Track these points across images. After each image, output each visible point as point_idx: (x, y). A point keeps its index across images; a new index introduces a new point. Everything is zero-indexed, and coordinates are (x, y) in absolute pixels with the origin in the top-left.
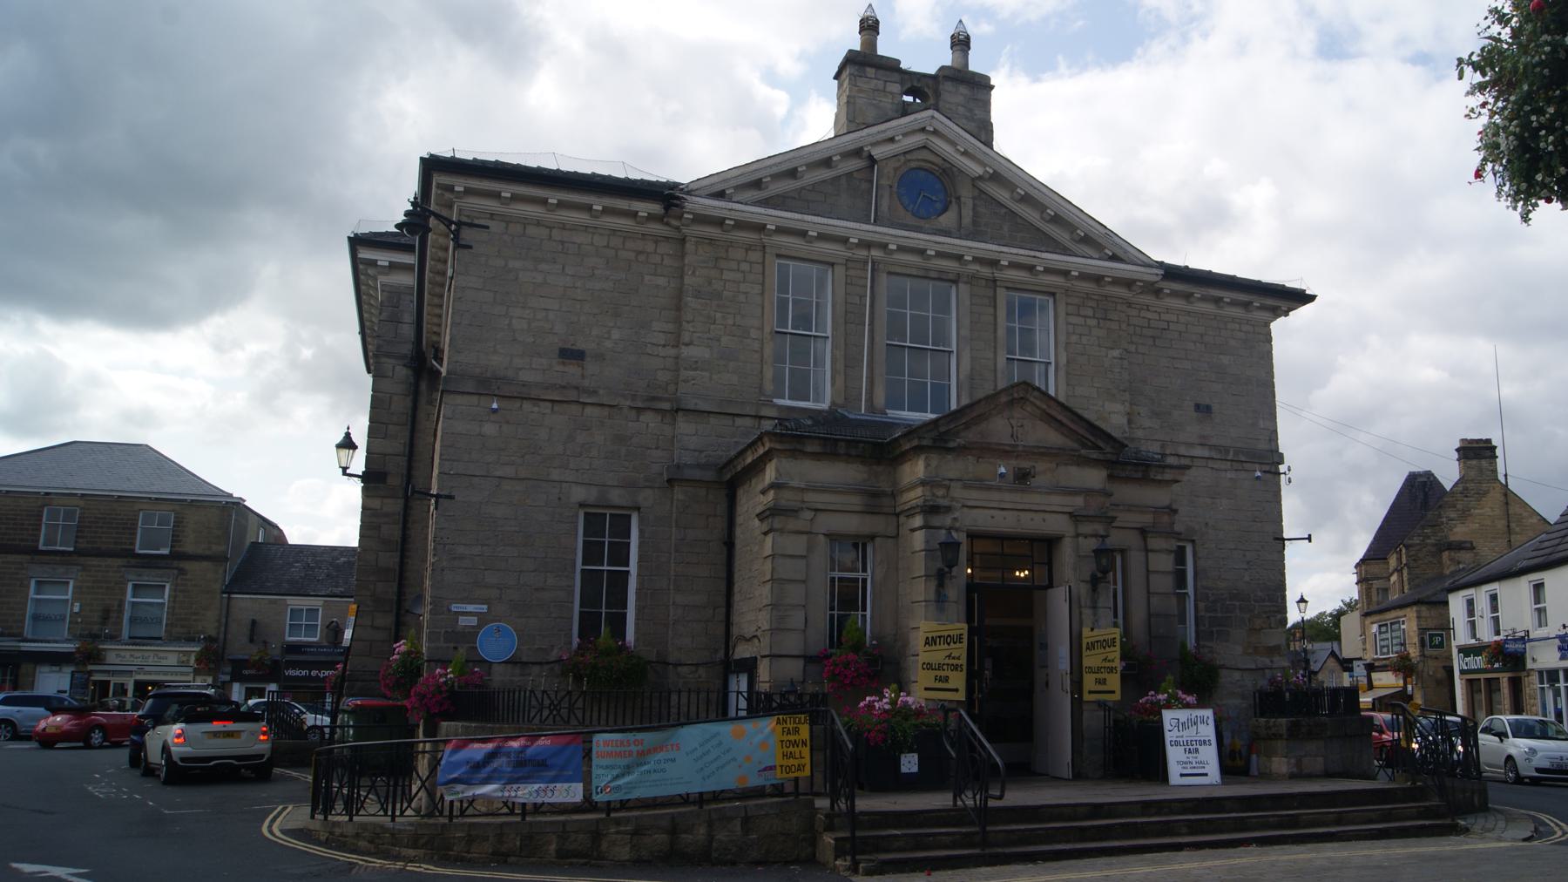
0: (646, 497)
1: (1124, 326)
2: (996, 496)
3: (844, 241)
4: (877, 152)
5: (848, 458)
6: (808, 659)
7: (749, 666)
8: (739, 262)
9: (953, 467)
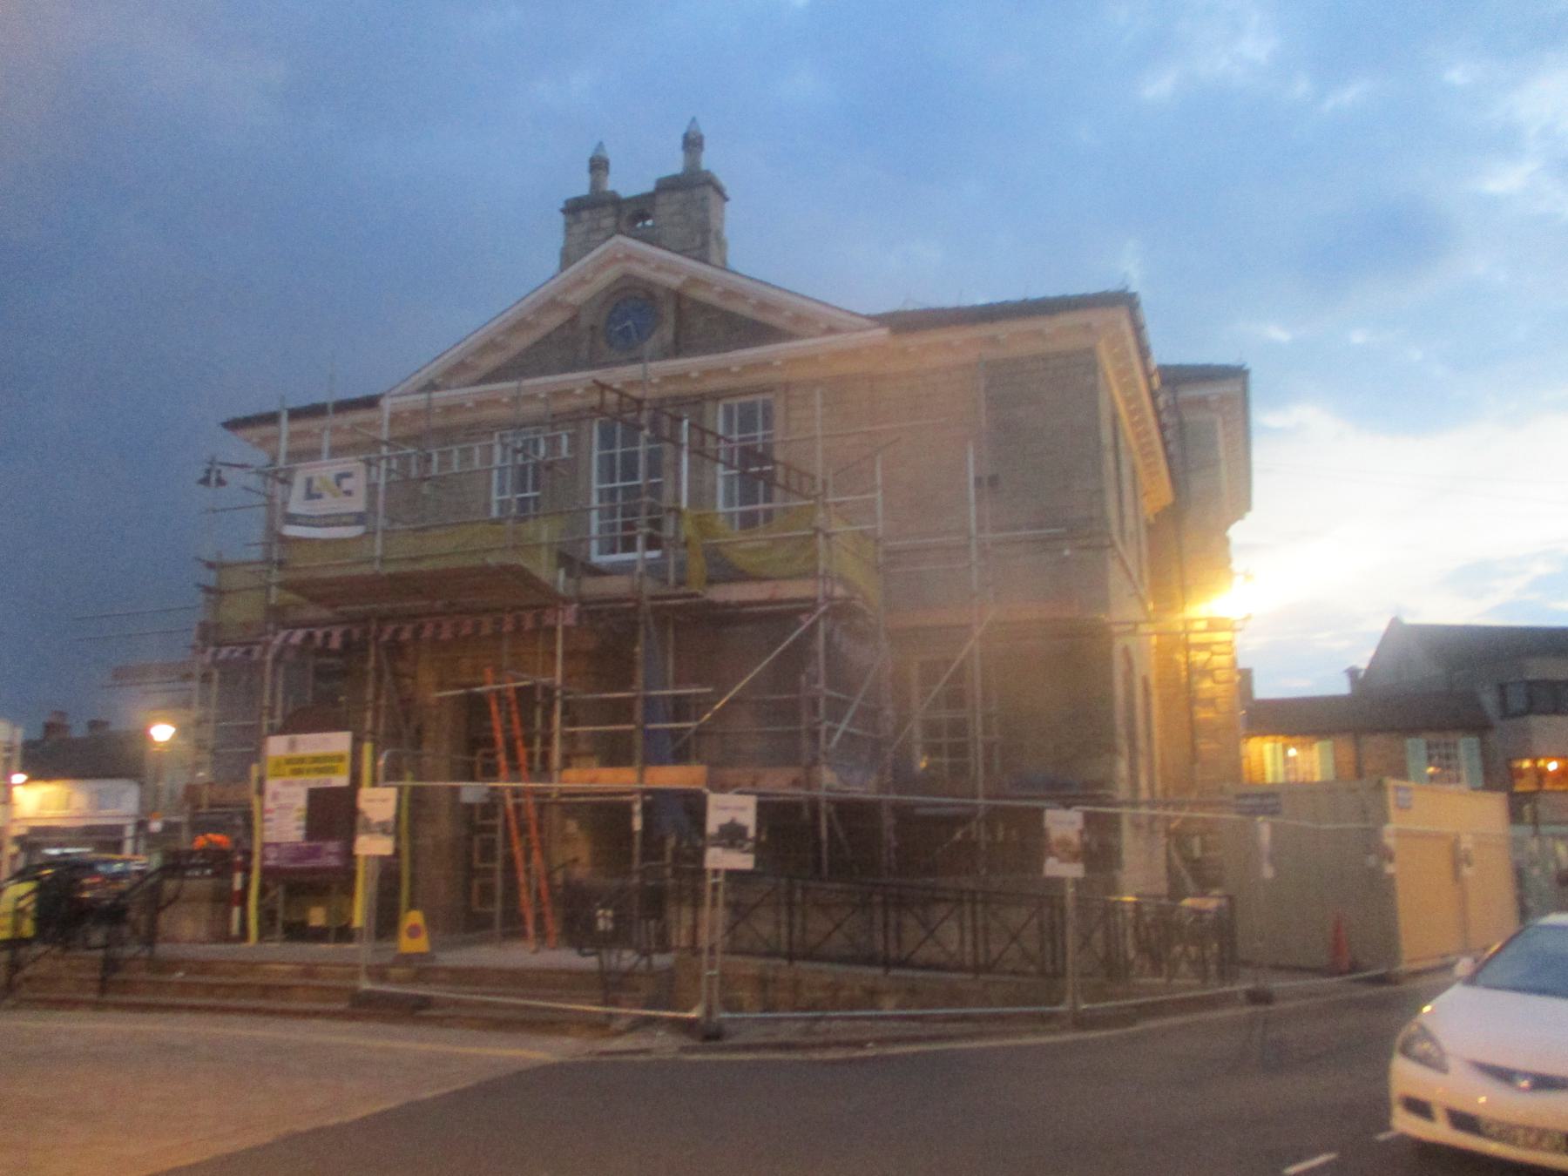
4: (570, 298)
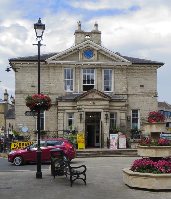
1: (126, 73)
2: (90, 106)
3: (74, 64)
4: (80, 49)
5: (69, 101)
6: (64, 131)
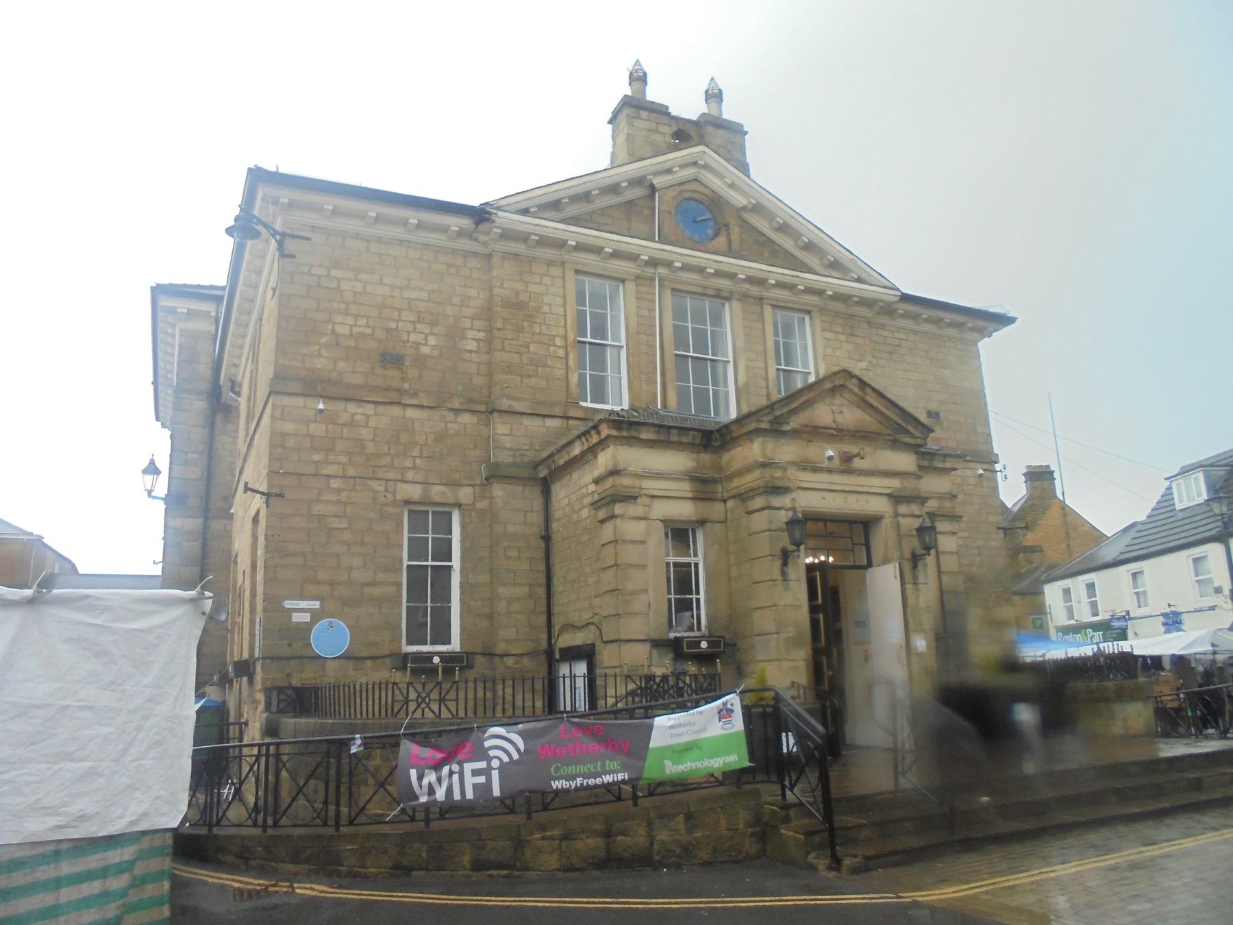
0: (465, 494)
1: (868, 342)
2: (825, 477)
3: (634, 258)
4: (657, 181)
5: (679, 446)
7: (586, 653)
8: (542, 276)
9: (787, 451)
